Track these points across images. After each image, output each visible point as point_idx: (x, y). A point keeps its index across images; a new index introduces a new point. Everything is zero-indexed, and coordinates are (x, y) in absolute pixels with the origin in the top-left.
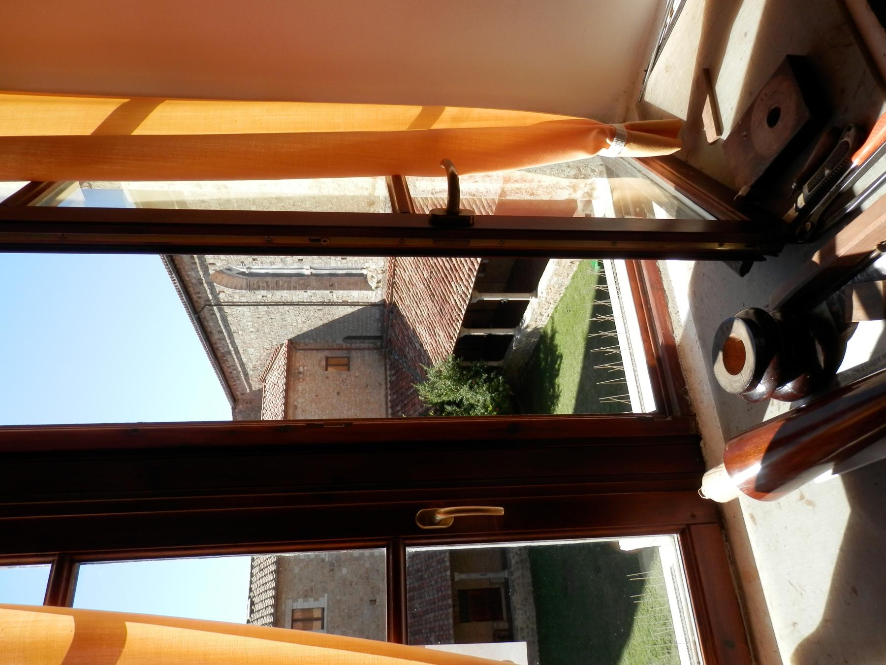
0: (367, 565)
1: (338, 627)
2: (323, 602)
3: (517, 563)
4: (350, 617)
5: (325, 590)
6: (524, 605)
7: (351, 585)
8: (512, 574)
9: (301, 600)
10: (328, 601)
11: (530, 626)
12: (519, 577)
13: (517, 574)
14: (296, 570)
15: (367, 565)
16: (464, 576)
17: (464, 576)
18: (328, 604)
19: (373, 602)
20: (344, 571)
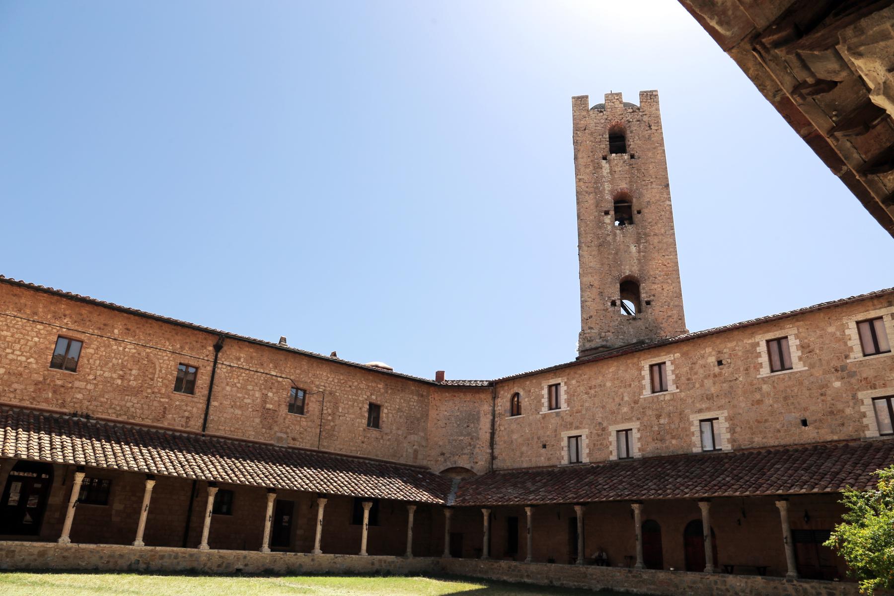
0: (848, 411)
1: (774, 387)
2: (798, 366)
4: (786, 398)
5: (812, 366)
7: (822, 395)
8: (790, 581)
9: (798, 342)
14: (831, 329)
15: (848, 411)
18: (796, 373)
19: (804, 423)
20: (837, 384)
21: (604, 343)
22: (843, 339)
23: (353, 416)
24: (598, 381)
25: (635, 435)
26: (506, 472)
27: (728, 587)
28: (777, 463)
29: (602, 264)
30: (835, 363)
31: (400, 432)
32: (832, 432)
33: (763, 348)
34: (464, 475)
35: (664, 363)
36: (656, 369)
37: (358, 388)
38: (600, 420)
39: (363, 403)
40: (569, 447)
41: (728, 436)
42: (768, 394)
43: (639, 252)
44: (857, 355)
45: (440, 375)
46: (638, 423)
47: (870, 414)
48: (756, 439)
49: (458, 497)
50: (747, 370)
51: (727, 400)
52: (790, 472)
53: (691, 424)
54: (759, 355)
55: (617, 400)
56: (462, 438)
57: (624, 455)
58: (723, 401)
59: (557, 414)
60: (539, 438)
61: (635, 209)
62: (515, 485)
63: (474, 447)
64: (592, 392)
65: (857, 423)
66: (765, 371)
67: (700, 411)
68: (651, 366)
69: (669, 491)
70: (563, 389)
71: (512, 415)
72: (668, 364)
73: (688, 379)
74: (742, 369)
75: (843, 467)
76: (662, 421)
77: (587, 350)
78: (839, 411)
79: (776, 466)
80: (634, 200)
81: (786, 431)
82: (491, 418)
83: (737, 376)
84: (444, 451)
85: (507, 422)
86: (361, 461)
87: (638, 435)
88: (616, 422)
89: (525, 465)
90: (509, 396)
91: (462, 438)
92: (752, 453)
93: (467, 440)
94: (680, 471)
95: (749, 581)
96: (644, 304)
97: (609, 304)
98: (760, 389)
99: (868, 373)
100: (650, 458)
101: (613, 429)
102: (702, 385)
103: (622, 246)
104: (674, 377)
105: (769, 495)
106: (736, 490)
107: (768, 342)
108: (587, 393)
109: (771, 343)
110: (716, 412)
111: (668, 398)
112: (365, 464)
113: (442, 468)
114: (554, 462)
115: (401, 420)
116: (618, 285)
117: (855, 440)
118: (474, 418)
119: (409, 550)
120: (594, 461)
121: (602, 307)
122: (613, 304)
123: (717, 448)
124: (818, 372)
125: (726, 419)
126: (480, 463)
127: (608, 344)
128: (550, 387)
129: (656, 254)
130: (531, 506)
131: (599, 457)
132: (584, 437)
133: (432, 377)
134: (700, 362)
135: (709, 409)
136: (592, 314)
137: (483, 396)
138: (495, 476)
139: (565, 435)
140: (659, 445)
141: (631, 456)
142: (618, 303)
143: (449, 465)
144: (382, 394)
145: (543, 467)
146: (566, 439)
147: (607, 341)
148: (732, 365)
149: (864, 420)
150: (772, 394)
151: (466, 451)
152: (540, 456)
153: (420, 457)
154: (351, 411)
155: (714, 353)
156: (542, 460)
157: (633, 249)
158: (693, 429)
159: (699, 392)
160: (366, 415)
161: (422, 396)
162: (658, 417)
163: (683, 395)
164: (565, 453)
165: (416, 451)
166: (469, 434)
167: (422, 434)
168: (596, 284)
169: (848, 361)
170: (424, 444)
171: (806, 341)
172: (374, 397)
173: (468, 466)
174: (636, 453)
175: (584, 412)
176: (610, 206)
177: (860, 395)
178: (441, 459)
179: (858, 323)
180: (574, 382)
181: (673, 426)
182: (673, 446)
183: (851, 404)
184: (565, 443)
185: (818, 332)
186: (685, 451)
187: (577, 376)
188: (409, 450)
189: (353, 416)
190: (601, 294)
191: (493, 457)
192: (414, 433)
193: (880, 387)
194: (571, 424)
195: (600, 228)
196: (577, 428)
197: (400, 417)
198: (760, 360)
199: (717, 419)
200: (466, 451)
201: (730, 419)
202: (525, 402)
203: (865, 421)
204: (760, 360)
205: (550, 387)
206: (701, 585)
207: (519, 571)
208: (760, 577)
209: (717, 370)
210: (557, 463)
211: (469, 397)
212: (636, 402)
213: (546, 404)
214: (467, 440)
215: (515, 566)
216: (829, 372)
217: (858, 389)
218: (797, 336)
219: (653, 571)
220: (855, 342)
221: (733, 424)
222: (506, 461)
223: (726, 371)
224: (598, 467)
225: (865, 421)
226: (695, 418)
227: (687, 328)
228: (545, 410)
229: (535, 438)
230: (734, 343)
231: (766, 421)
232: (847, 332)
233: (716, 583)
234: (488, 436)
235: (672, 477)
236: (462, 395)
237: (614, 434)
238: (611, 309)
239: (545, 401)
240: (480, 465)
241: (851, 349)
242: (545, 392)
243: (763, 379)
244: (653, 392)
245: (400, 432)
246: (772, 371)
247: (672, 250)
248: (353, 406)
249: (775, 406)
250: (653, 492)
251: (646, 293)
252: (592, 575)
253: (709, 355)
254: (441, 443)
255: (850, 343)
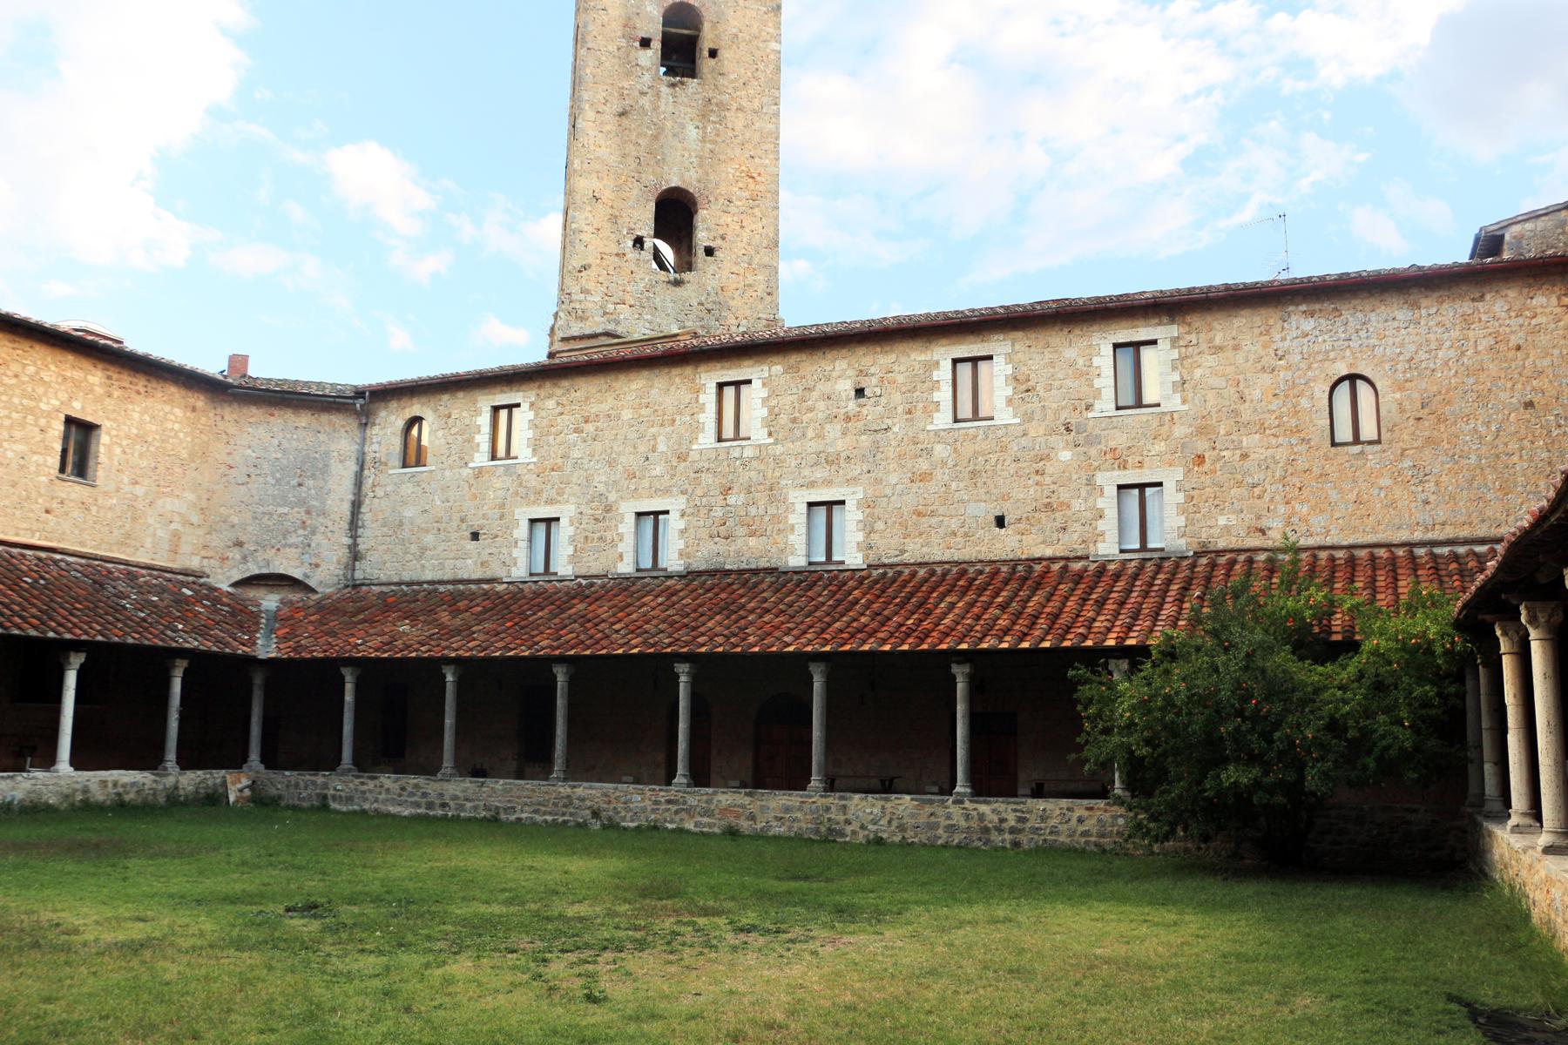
0: (1077, 505)
3: (982, 817)
5: (1028, 417)
6: (890, 822)
8: (958, 802)
9: (1009, 370)
10: (1006, 426)
11: (849, 829)
12: (949, 817)
13: (955, 810)
14: (1070, 353)
16: (961, 687)
17: (961, 687)
18: (998, 427)
19: (1000, 522)
20: (1066, 455)
21: (611, 327)
22: (1087, 374)
23: (20, 447)
24: (605, 407)
25: (673, 525)
26: (384, 589)
27: (850, 816)
28: (949, 592)
29: (624, 156)
30: (1064, 415)
31: (139, 491)
32: (1044, 542)
33: (944, 373)
34: (295, 596)
35: (749, 382)
36: (729, 392)
37: (36, 379)
38: (601, 488)
39: (49, 415)
40: (530, 540)
41: (860, 537)
42: (944, 463)
43: (703, 140)
44: (1105, 405)
45: (239, 362)
46: (683, 499)
47: (1111, 513)
48: (910, 547)
49: (285, 638)
50: (910, 412)
51: (865, 468)
52: (975, 610)
53: (790, 508)
54: (936, 385)
55: (642, 449)
56: (286, 510)
57: (647, 563)
58: (857, 469)
59: (507, 467)
60: (462, 520)
61: (706, 44)
62: (411, 616)
63: (313, 532)
64: (590, 428)
65: (1087, 528)
66: (943, 419)
67: (812, 485)
68: (721, 386)
69: (752, 639)
70: (522, 417)
71: (404, 466)
72: (756, 384)
73: (794, 420)
74: (900, 409)
75: (1064, 605)
76: (731, 500)
77: (574, 338)
78: (1062, 504)
79: (948, 599)
80: (706, 27)
81: (966, 535)
82: (355, 468)
83: (889, 422)
84: (243, 538)
85: (390, 479)
86: (43, 555)
87: (681, 525)
88: (635, 494)
89: (429, 575)
90: (400, 423)
91: (286, 510)
92: (900, 573)
93: (297, 514)
94: (765, 600)
95: (889, 805)
96: (701, 252)
97: (630, 243)
98: (929, 452)
99: (1119, 440)
100: (700, 573)
101: (628, 509)
102: (820, 436)
103: (669, 124)
104: (765, 412)
105: (943, 651)
106: (884, 641)
107: (955, 361)
108: (576, 431)
109: (959, 365)
110: (843, 490)
111: (748, 453)
112: (56, 562)
113: (237, 577)
114: (496, 570)
115: (144, 463)
116: (652, 206)
117: (1080, 558)
118: (312, 468)
119: (171, 755)
120: (583, 572)
121: (613, 248)
122: (639, 242)
123: (835, 558)
124: (1037, 429)
125: (859, 505)
126: (324, 566)
127: (620, 330)
128: (496, 409)
129: (738, 151)
130: (457, 661)
131: (594, 565)
132: (564, 522)
133: (213, 365)
134: (823, 387)
135: (828, 483)
136: (590, 260)
137: (337, 419)
138: (360, 601)
139: (523, 514)
140: (722, 547)
141: (662, 564)
142: (648, 244)
143: (254, 570)
144: (97, 400)
145: (469, 581)
146: (524, 525)
147: (618, 323)
148: (883, 400)
149: (1100, 522)
150: (950, 463)
151: (293, 539)
152: (466, 556)
153: (185, 548)
154: (17, 434)
155: (851, 372)
156: (469, 564)
157: (692, 132)
158: (793, 519)
159: (813, 446)
160: (58, 447)
161: (194, 409)
162: (726, 491)
163: (779, 449)
164: (520, 553)
165: (176, 535)
166: (302, 502)
167: (190, 497)
168: (607, 195)
169: (1090, 415)
170: (195, 519)
171: (1024, 369)
172: (77, 405)
173: (297, 573)
174: (672, 560)
175: (569, 469)
176: (655, 30)
177: (1100, 478)
178: (235, 554)
179: (1116, 346)
180: (551, 404)
181: (753, 511)
182: (747, 551)
183: (1083, 494)
184: (522, 531)
185: (1047, 355)
186: (774, 563)
187: (559, 392)
188: (160, 533)
189: (20, 447)
190: (614, 219)
191: (355, 555)
192: (171, 494)
193: (1134, 467)
194: (539, 493)
195: (628, 74)
196: (550, 502)
197: (141, 455)
198: (936, 396)
199: (842, 502)
200: (293, 539)
201: (868, 504)
202: (427, 434)
203: (1101, 525)
204: (936, 396)
205: (496, 409)
206: (799, 815)
207: (424, 795)
208: (908, 797)
209: (852, 406)
210: (500, 573)
211: (304, 419)
212: (682, 458)
213: (485, 447)
214: (297, 514)
215: (416, 786)
216: (1053, 431)
217: (1098, 468)
218: (1009, 359)
219: (710, 790)
220: (1105, 382)
221: (871, 515)
222: (386, 564)
223: (870, 411)
224: (592, 585)
225: (1101, 525)
226: (799, 499)
227: (781, 314)
228: (481, 458)
229: (456, 517)
230: (892, 357)
231: (933, 514)
232: (1096, 361)
233: (828, 809)
234: (346, 508)
235: (752, 611)
236: (289, 415)
237: (631, 519)
238: (632, 254)
239: (483, 439)
240: (324, 571)
241: (1098, 394)
242: (484, 419)
243: (936, 433)
244: (720, 440)
245: (139, 491)
246: (956, 421)
247: (769, 146)
248: (23, 425)
249: (954, 485)
250: (720, 640)
251: (708, 229)
252: (583, 800)
253: (840, 372)
254: (236, 520)
255: (1097, 383)
